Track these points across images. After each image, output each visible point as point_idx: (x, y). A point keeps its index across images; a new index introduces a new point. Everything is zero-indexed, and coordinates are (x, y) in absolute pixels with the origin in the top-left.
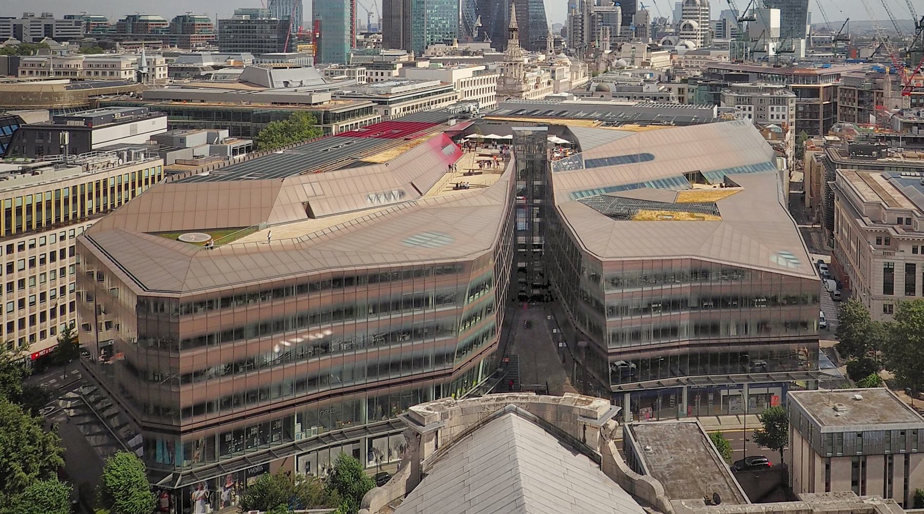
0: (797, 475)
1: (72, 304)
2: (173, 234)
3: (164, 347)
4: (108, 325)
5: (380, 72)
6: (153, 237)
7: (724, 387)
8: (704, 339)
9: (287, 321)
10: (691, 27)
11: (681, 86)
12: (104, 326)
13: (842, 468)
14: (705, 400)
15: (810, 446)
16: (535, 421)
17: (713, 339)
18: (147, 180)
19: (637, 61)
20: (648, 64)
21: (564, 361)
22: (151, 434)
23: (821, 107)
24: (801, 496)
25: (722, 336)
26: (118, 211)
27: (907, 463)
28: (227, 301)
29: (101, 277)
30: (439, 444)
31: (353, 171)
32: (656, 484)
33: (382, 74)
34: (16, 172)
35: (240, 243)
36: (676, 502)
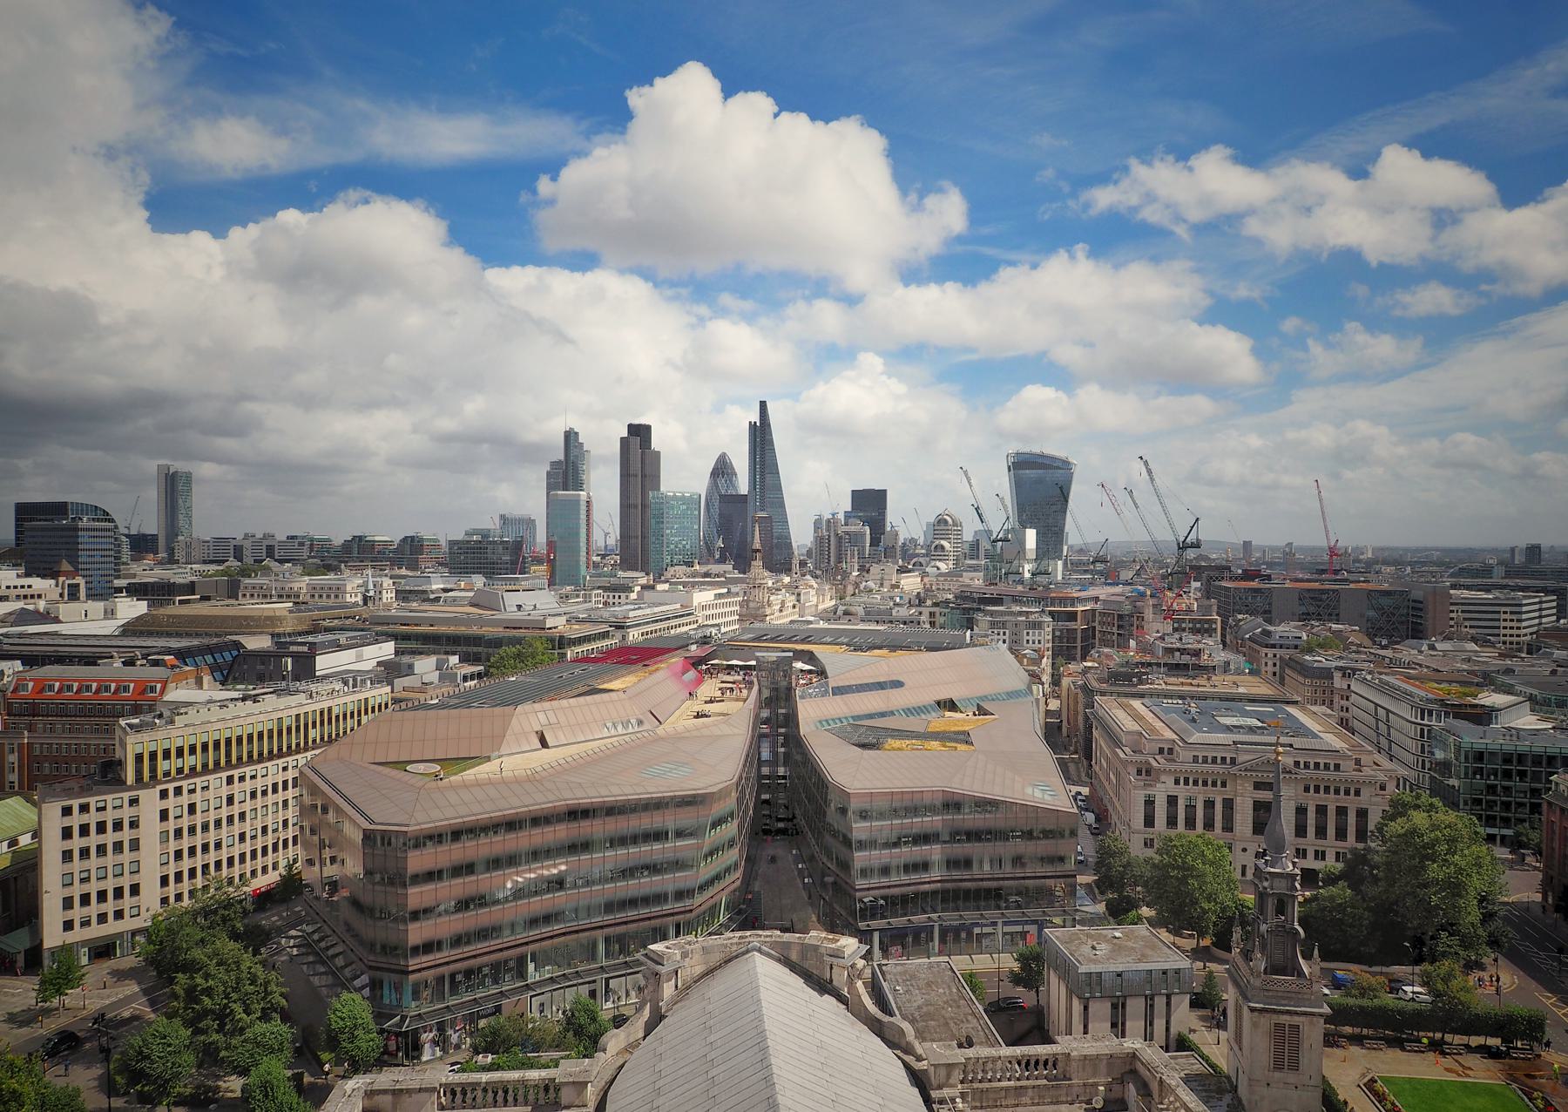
0: (1054, 1016)
1: (295, 838)
2: (400, 765)
3: (392, 882)
4: (333, 860)
5: (617, 595)
6: (380, 768)
7: (977, 925)
8: (956, 874)
9: (520, 856)
10: (943, 548)
11: (932, 610)
12: (328, 861)
13: (1100, 1009)
14: (957, 938)
15: (1067, 987)
16: (779, 961)
17: (965, 874)
18: (373, 708)
19: (887, 583)
20: (898, 587)
21: (810, 898)
22: (378, 974)
23: (1079, 632)
24: (1058, 1038)
25: (975, 872)
26: (343, 740)
27: (1168, 1004)
28: (457, 834)
29: (325, 810)
30: (679, 985)
31: (589, 698)
32: (906, 1026)
33: (620, 597)
34: (236, 699)
35: (471, 774)
36: (927, 1045)
